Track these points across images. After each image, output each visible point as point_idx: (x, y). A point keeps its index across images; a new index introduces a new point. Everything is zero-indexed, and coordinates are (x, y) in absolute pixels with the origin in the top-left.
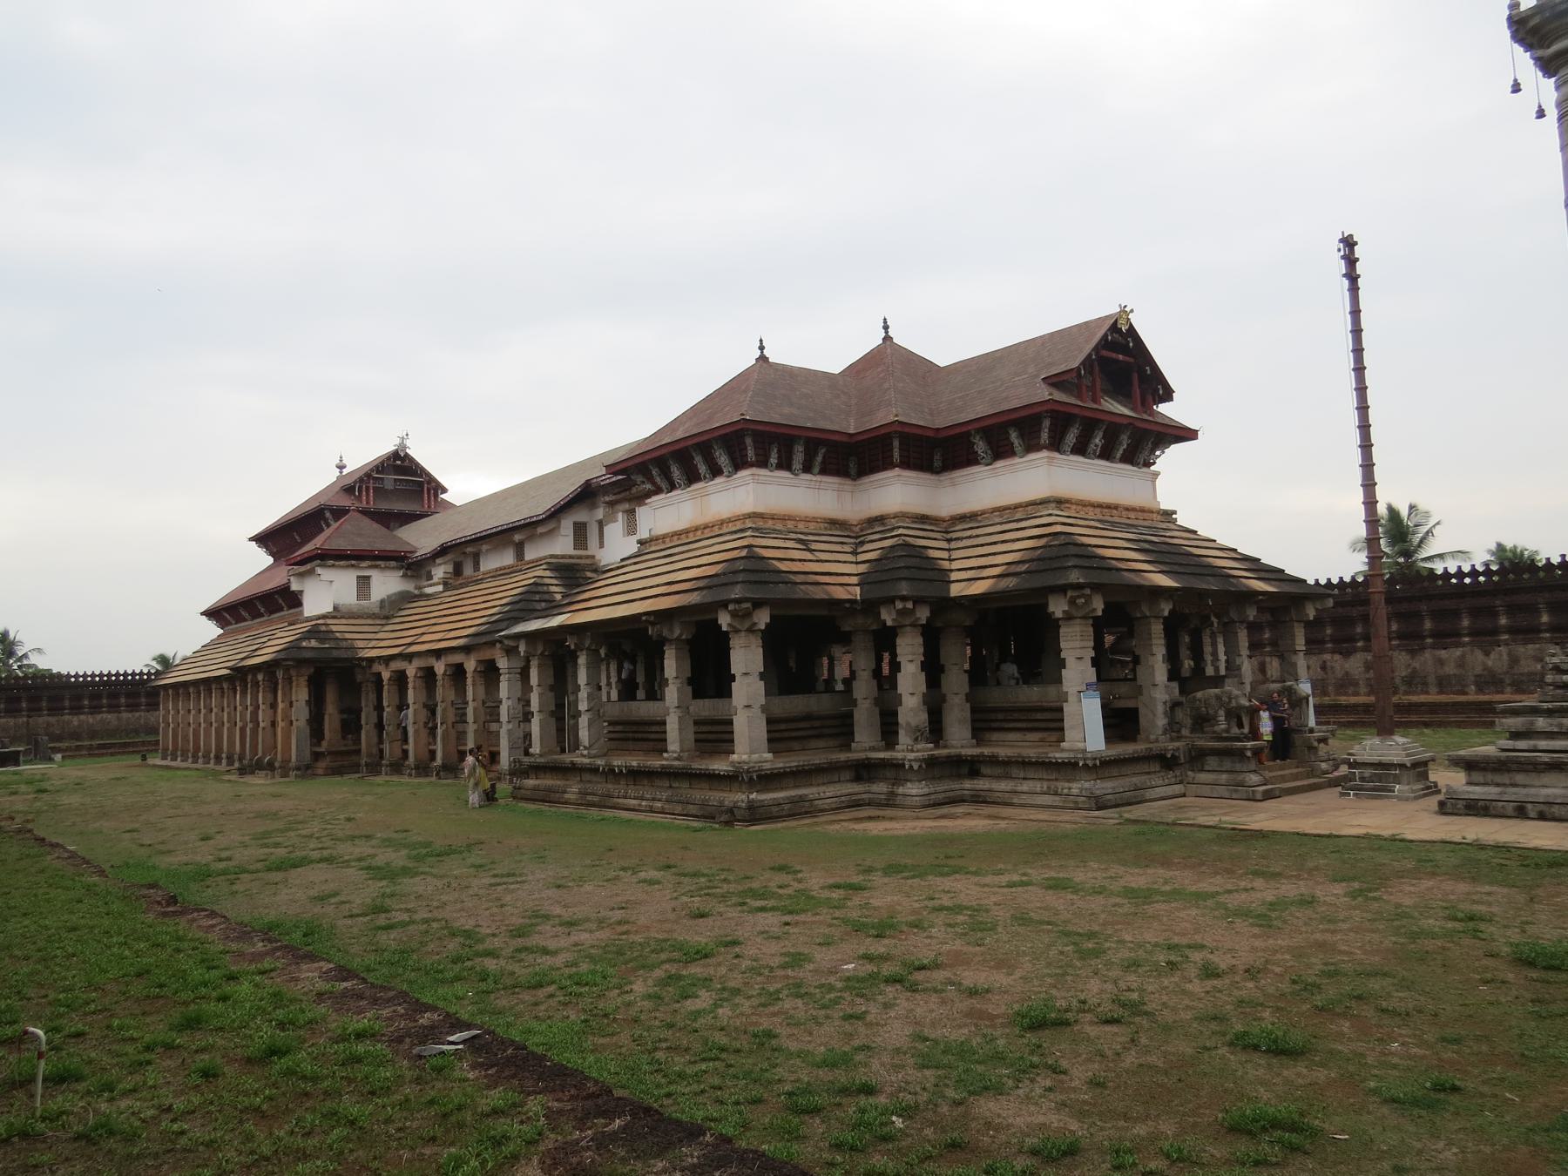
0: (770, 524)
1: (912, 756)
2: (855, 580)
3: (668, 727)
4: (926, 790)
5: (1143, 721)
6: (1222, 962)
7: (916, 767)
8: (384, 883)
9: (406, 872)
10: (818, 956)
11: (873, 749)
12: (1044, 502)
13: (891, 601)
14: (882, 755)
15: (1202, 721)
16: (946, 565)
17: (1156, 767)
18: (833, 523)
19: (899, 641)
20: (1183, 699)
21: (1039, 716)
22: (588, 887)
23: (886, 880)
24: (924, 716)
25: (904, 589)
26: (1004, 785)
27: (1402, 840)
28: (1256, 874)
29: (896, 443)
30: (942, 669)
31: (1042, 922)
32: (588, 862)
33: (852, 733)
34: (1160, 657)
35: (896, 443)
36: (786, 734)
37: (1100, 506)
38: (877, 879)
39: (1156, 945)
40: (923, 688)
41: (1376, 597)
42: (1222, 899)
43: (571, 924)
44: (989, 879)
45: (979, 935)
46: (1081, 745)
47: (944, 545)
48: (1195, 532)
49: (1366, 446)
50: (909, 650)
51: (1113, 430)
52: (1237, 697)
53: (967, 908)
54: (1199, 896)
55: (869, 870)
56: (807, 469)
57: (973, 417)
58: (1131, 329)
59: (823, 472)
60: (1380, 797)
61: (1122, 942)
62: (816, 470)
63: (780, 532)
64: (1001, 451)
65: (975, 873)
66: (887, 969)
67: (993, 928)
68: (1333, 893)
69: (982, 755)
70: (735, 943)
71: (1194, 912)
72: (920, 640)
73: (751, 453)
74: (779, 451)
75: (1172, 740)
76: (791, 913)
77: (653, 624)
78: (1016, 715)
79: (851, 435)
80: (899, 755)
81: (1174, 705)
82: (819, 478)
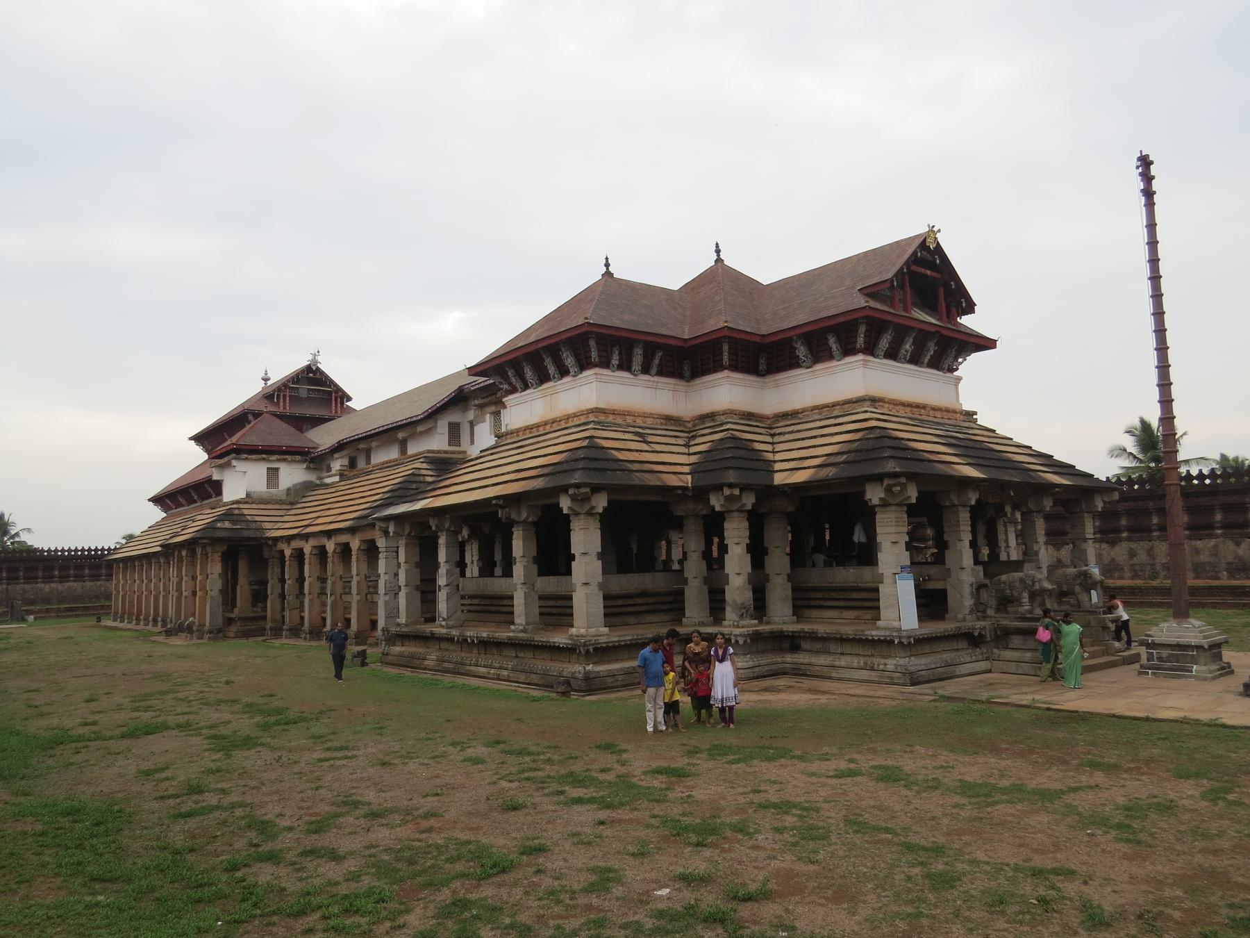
0: (611, 418)
1: (737, 631)
2: (687, 469)
3: (516, 602)
4: (751, 664)
5: (950, 600)
6: (1108, 903)
7: (741, 642)
8: (217, 756)
9: (248, 743)
10: (629, 874)
11: (702, 624)
13: (719, 488)
15: (1006, 602)
16: (770, 456)
17: (963, 644)
18: (668, 419)
19: (726, 525)
20: (987, 582)
22: (412, 766)
23: (711, 764)
24: (749, 595)
25: (731, 477)
26: (823, 660)
27: (1224, 726)
28: (1094, 766)
29: (726, 347)
31: (877, 829)
32: (423, 735)
33: (683, 609)
34: (967, 544)
35: (726, 347)
36: (623, 610)
37: (910, 405)
38: (703, 763)
39: (1016, 869)
40: (749, 569)
41: (1173, 489)
42: (1069, 799)
43: (374, 815)
44: (816, 766)
45: (811, 845)
47: (769, 439)
48: (994, 431)
49: (1162, 349)
50: (736, 534)
51: (923, 336)
52: (1040, 581)
54: (1045, 796)
56: (646, 370)
58: (939, 249)
59: (660, 373)
60: (1179, 677)
61: (974, 862)
62: (654, 371)
63: (619, 425)
64: (820, 354)
65: (800, 758)
66: (709, 899)
68: (1188, 793)
69: (803, 631)
70: (540, 850)
71: (1044, 818)
72: (746, 524)
73: (594, 355)
74: (620, 354)
75: (978, 619)
76: (609, 806)
77: (502, 507)
78: (833, 594)
79: (685, 340)
81: (980, 587)
82: (656, 379)
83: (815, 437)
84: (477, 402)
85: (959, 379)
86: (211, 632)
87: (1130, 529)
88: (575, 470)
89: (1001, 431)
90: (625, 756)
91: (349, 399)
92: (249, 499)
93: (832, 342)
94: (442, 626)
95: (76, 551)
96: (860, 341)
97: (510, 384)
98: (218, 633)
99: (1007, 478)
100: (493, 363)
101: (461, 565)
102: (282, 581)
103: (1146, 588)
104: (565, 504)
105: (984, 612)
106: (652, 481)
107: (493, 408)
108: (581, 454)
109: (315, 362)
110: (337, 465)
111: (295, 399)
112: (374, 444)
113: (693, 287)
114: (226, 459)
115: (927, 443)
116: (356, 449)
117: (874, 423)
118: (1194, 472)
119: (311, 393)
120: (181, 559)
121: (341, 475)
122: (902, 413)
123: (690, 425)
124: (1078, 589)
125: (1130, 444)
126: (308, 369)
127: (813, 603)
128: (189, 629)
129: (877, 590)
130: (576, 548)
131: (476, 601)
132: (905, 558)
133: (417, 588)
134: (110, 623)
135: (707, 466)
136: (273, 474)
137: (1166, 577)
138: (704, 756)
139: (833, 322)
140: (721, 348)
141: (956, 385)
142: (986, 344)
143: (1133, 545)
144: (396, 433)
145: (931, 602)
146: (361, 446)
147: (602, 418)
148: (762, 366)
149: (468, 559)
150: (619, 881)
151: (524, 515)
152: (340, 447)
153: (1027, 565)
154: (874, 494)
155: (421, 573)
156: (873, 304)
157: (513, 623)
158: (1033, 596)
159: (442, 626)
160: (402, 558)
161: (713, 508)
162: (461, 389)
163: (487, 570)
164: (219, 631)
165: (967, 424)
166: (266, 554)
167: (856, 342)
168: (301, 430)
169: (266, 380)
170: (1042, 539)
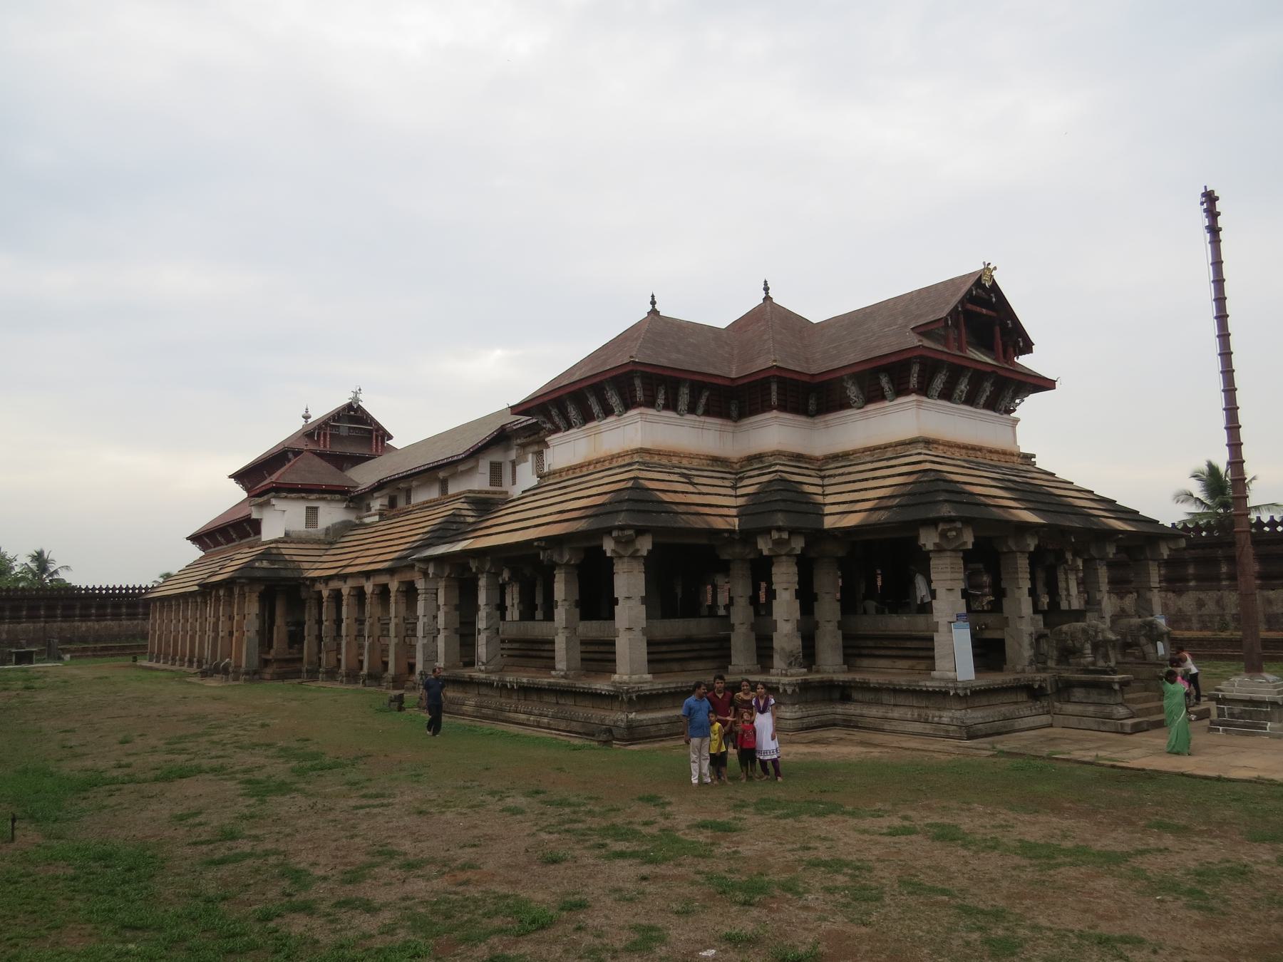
1: (785, 680)
2: (734, 512)
4: (799, 714)
7: (789, 691)
8: (252, 801)
9: (283, 788)
11: (749, 672)
12: (912, 442)
13: (767, 531)
15: (1067, 653)
16: (820, 499)
17: (1023, 697)
18: (715, 460)
19: (774, 570)
20: (1047, 631)
21: (909, 644)
22: (449, 815)
23: (758, 819)
24: (797, 643)
25: (780, 520)
26: (874, 711)
28: (1163, 827)
29: (774, 387)
30: (814, 598)
31: (933, 890)
33: (730, 656)
34: (1026, 591)
35: (774, 387)
38: (750, 818)
39: (1081, 936)
40: (797, 615)
42: (1137, 862)
43: (410, 866)
44: (867, 823)
45: (864, 906)
47: (818, 481)
49: (1230, 390)
50: (784, 579)
51: (979, 376)
52: (1103, 631)
53: (847, 865)
55: (741, 806)
56: (692, 410)
57: (845, 363)
58: (995, 288)
59: (707, 413)
60: (1253, 734)
61: (1035, 927)
62: (700, 411)
63: (665, 466)
64: (873, 395)
65: (852, 814)
67: (878, 899)
69: (854, 681)
70: (581, 906)
71: (1110, 882)
72: (796, 569)
73: (639, 394)
75: (1038, 670)
76: (652, 861)
77: (544, 549)
78: (886, 643)
79: (732, 379)
80: (774, 679)
81: (1040, 637)
82: (703, 419)
83: (866, 480)
84: (519, 441)
85: (1016, 421)
86: (247, 673)
87: (1198, 578)
88: (617, 512)
89: (1061, 475)
90: (668, 809)
91: (390, 437)
92: (288, 538)
93: (884, 381)
94: (481, 671)
95: (114, 589)
96: (914, 381)
97: (553, 423)
98: (254, 675)
99: (1068, 523)
100: (537, 402)
101: (502, 608)
102: (320, 622)
103: (1215, 640)
104: (609, 546)
105: (1045, 663)
106: (698, 523)
107: (536, 448)
108: (626, 496)
109: (356, 400)
110: (376, 505)
111: (336, 438)
112: (414, 483)
113: (738, 325)
114: (265, 498)
115: (983, 486)
116: (395, 489)
117: (928, 466)
118: (1265, 518)
119: (352, 431)
120: (218, 599)
121: (381, 515)
122: (957, 455)
123: (737, 466)
124: (1143, 640)
125: (1197, 489)
126: (349, 407)
127: (865, 652)
128: (225, 671)
129: (932, 639)
130: (619, 592)
131: (515, 646)
132: (961, 606)
133: (456, 631)
134: (146, 663)
135: (754, 509)
136: (312, 513)
137: (1236, 629)
138: (751, 809)
139: (884, 362)
140: (770, 388)
141: (1014, 427)
142: (1045, 384)
143: (1202, 596)
144: (438, 472)
145: (988, 652)
146: (401, 485)
147: (647, 458)
148: (812, 407)
149: (508, 602)
150: (662, 940)
151: (566, 558)
152: (380, 486)
153: (1089, 615)
154: (929, 540)
155: (461, 616)
156: (927, 343)
157: (554, 669)
158: (1096, 647)
159: (481, 671)
160: (441, 601)
161: (761, 551)
162: (503, 428)
163: (528, 613)
164: (255, 673)
165: (1025, 468)
166: (304, 595)
167: (909, 382)
168: (341, 469)
169: (306, 417)
170: (1105, 587)
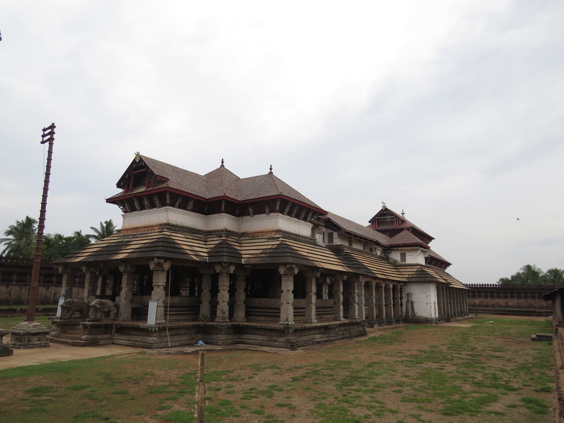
14: (211, 323)
29: (223, 203)
35: (223, 203)
46: (286, 323)
104: (152, 266)
127: (253, 313)
161: (215, 270)
